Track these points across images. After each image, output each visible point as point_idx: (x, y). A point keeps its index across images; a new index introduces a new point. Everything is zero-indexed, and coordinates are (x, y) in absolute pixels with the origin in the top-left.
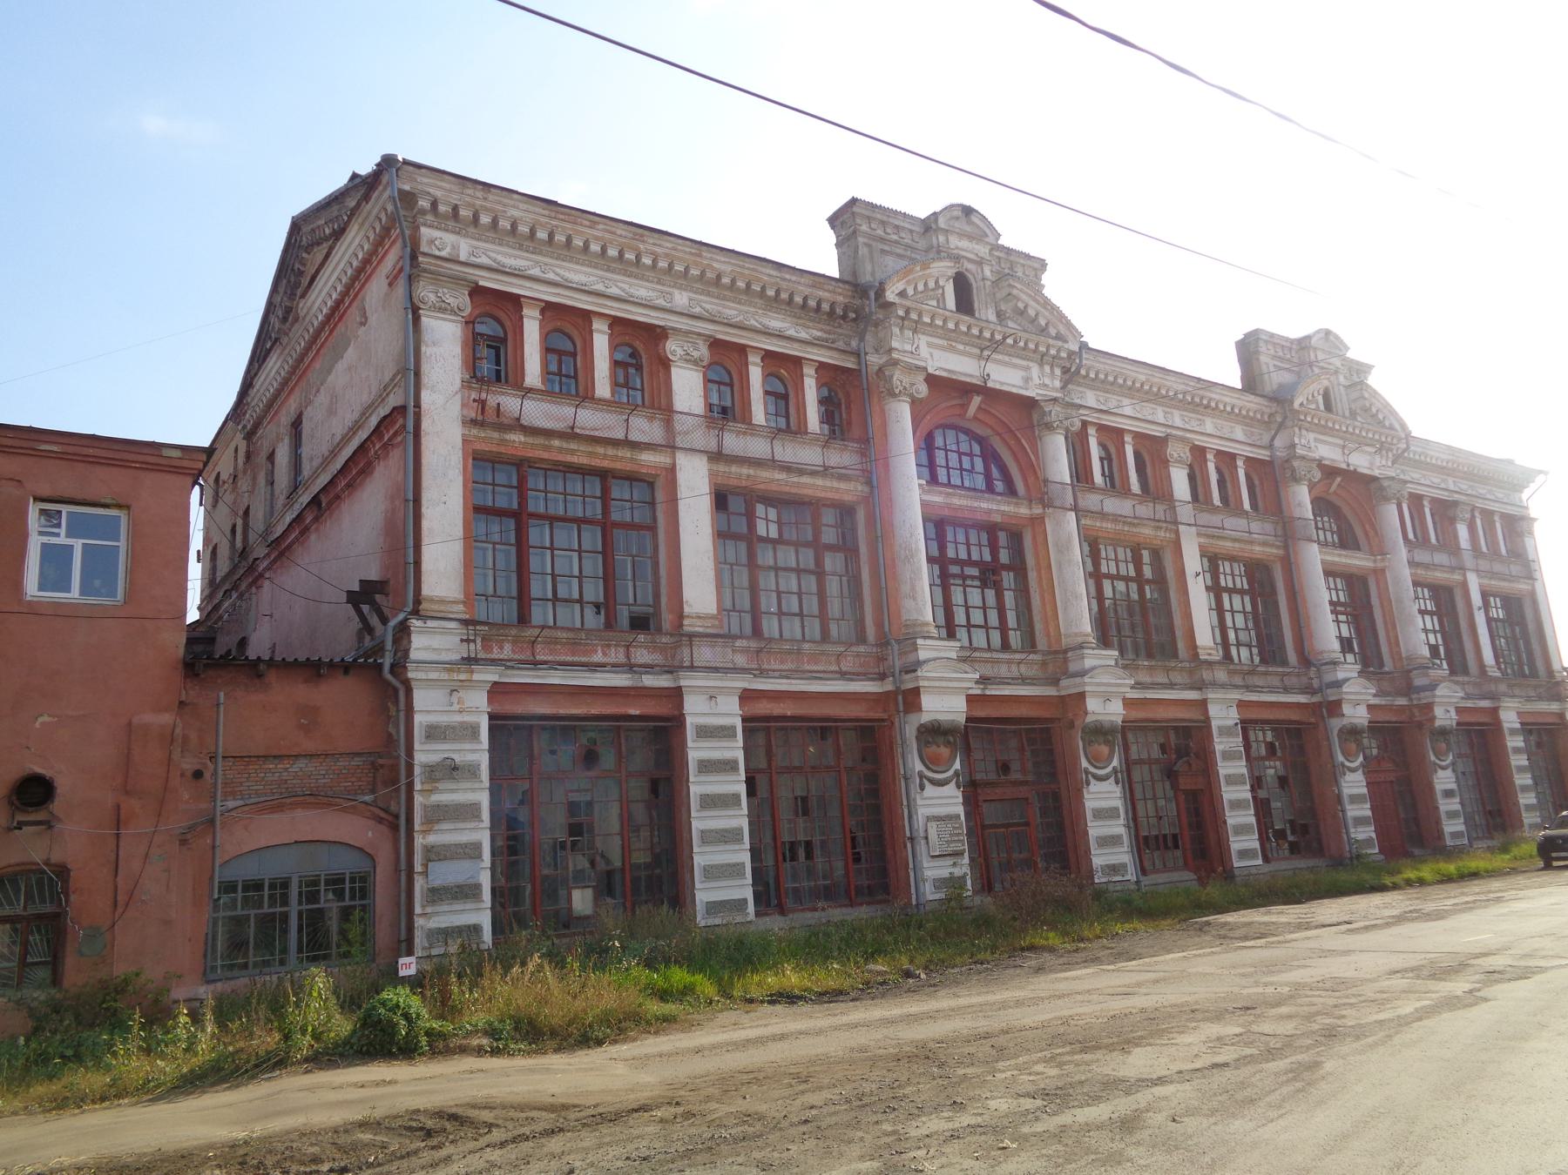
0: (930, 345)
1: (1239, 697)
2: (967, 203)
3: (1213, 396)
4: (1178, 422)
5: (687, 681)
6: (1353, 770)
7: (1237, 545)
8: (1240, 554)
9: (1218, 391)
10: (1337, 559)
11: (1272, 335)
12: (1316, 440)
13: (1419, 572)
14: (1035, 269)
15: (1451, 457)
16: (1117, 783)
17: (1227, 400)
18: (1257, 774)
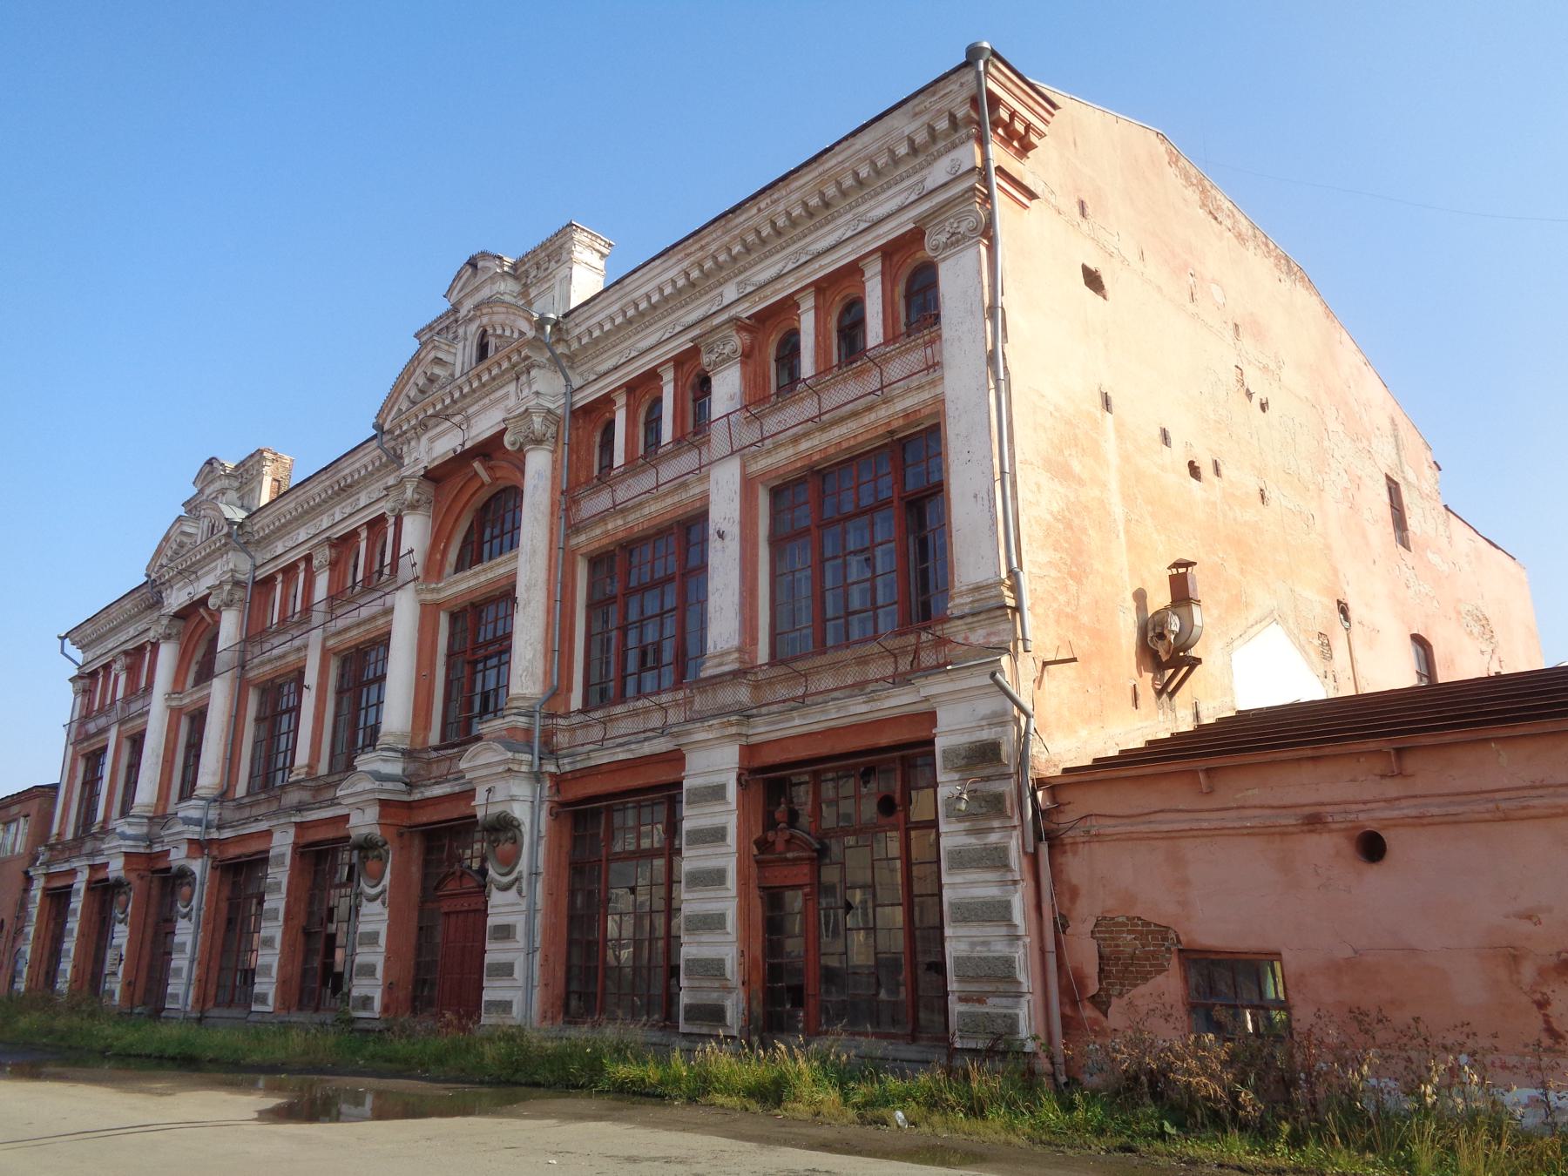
0: (180, 589)
1: (298, 819)
2: (203, 463)
3: (344, 473)
4: (338, 517)
5: (76, 864)
6: (372, 899)
7: (362, 629)
8: (367, 637)
9: (345, 464)
10: (473, 582)
11: (430, 327)
12: (432, 440)
13: (610, 526)
14: (258, 461)
15: (686, 264)
16: (190, 920)
17: (357, 465)
18: (331, 903)
